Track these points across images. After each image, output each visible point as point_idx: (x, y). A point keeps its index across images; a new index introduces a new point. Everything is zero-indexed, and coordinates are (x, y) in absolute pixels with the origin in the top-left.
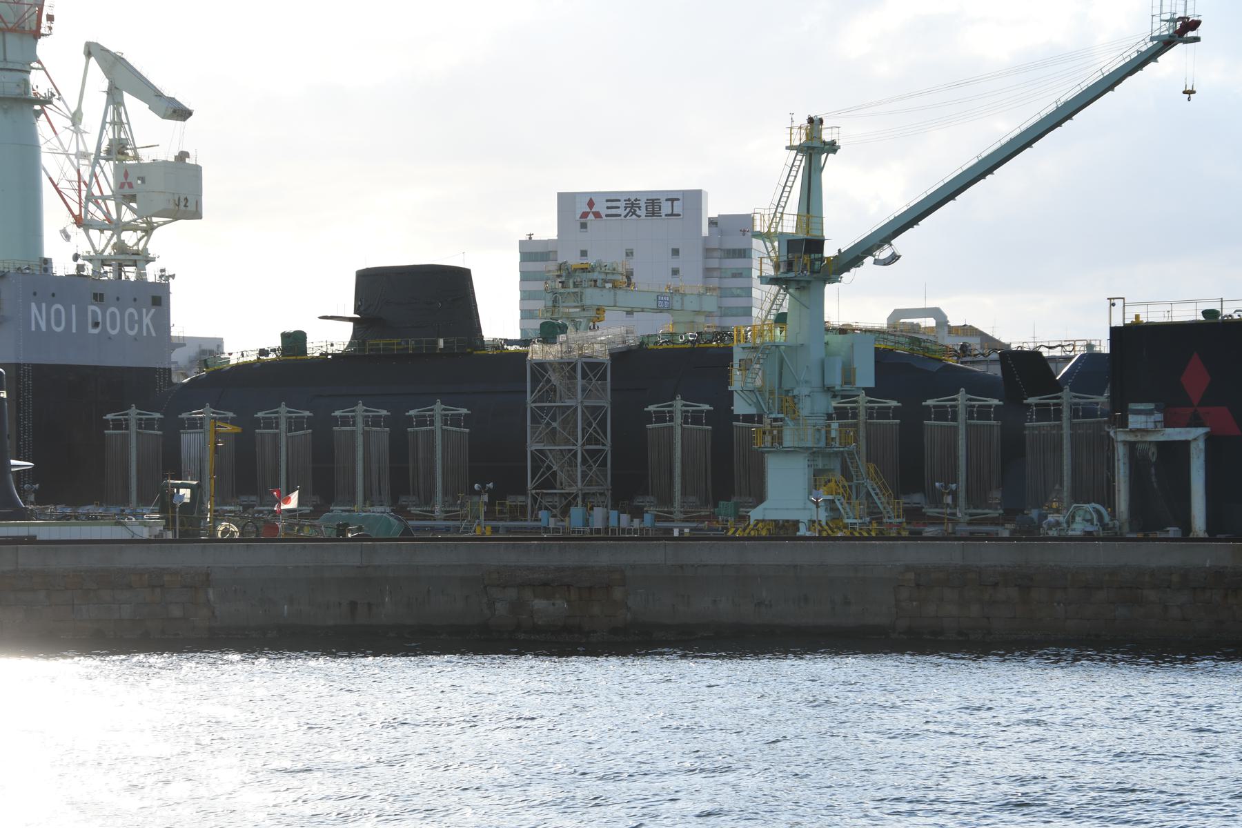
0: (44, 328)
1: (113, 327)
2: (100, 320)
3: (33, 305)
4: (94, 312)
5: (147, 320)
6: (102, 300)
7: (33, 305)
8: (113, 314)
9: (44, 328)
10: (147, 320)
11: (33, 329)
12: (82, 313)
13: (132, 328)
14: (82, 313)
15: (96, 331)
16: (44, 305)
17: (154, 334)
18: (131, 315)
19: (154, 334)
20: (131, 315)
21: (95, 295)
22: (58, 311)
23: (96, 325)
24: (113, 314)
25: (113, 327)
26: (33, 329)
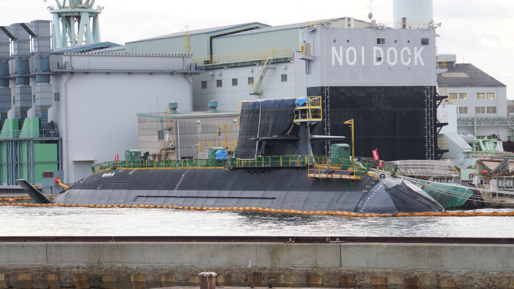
0: (341, 63)
1: (392, 60)
2: (382, 56)
3: (334, 49)
4: (378, 51)
5: (417, 55)
6: (383, 43)
7: (334, 49)
8: (392, 52)
9: (341, 63)
10: (417, 55)
11: (333, 63)
12: (369, 53)
13: (406, 60)
14: (369, 53)
15: (379, 63)
16: (341, 48)
17: (423, 64)
18: (405, 52)
19: (423, 64)
20: (405, 52)
21: (379, 41)
22: (351, 52)
23: (379, 59)
24: (392, 52)
25: (392, 60)
26: (333, 63)
